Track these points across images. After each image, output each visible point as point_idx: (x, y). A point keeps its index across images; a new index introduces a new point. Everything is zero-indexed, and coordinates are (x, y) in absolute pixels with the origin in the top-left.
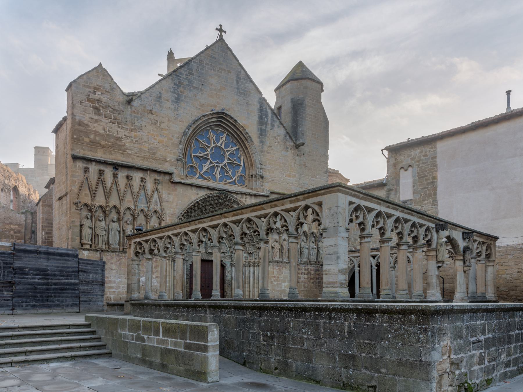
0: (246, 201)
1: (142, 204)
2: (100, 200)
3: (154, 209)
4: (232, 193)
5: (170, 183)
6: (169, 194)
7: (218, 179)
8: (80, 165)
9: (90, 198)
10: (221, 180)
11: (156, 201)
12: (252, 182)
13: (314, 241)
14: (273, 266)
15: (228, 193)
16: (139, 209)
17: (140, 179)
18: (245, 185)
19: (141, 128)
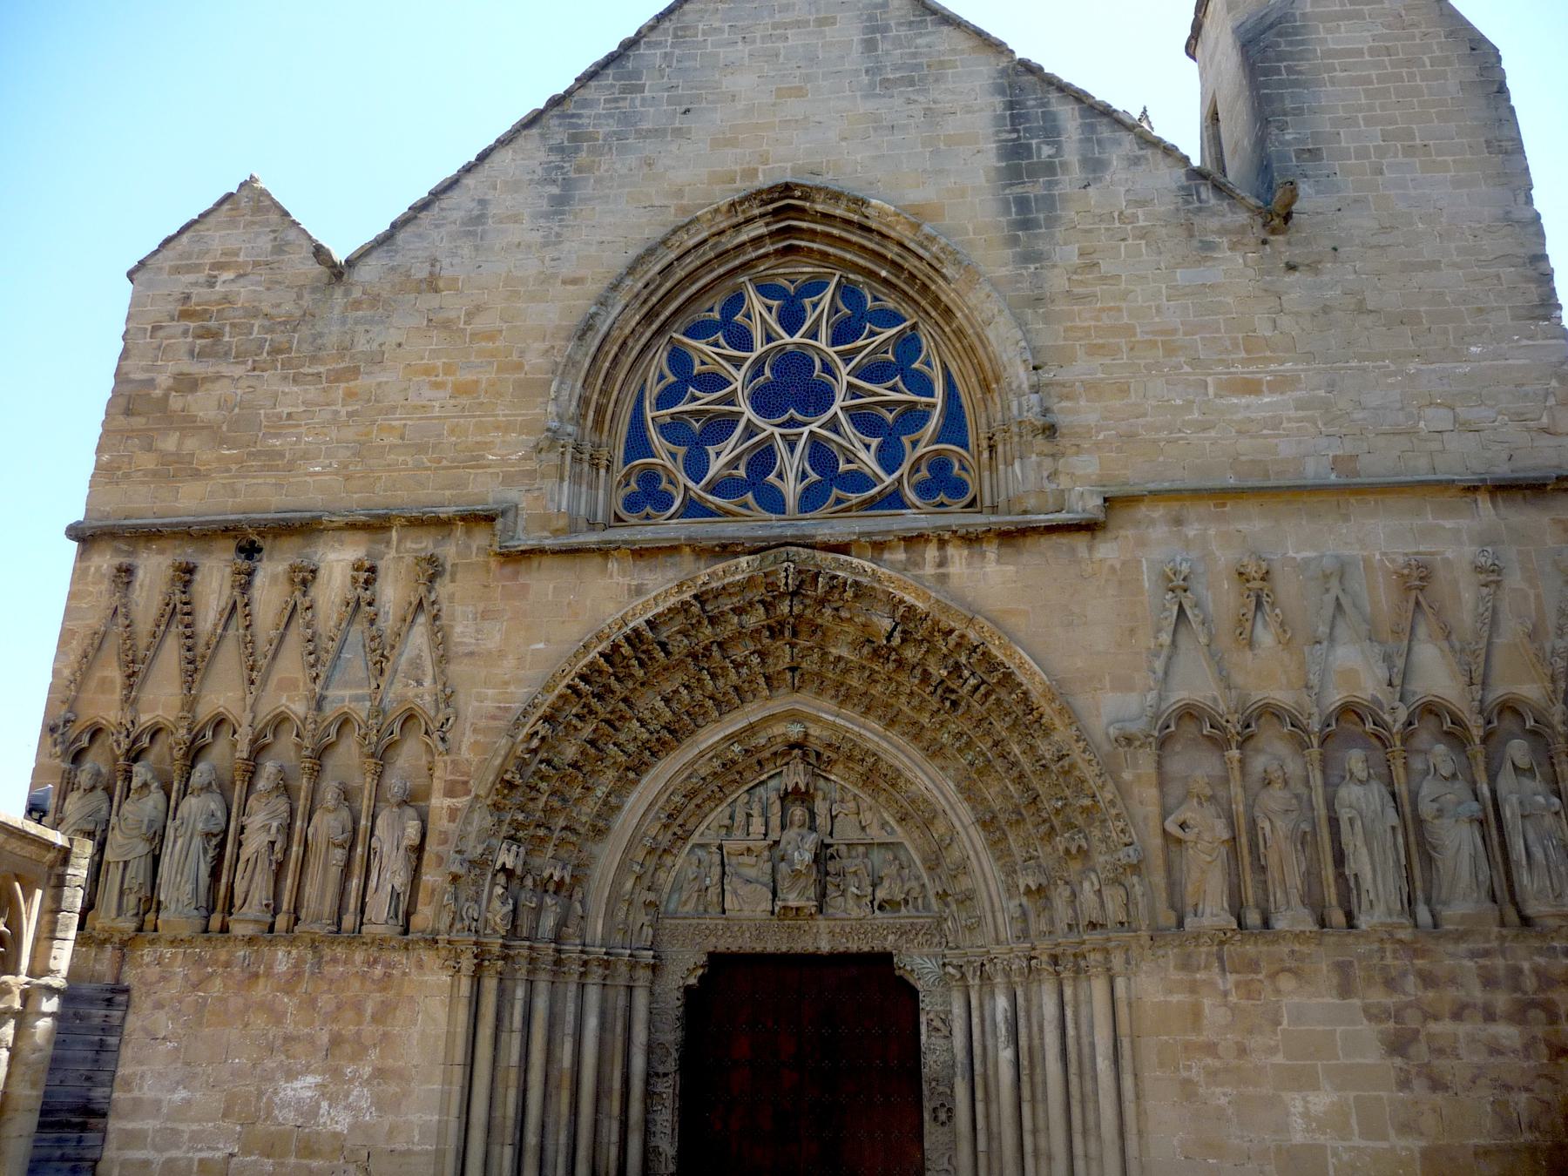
0: (943, 578)
1: (346, 685)
2: (162, 700)
3: (402, 699)
4: (843, 548)
5: (493, 563)
6: (485, 615)
7: (791, 502)
8: (105, 561)
9: (118, 694)
10: (811, 499)
11: (416, 663)
12: (992, 469)
13: (1523, 763)
14: (1186, 965)
15: (819, 555)
16: (330, 711)
17: (350, 572)
18: (968, 499)
19: (376, 359)
